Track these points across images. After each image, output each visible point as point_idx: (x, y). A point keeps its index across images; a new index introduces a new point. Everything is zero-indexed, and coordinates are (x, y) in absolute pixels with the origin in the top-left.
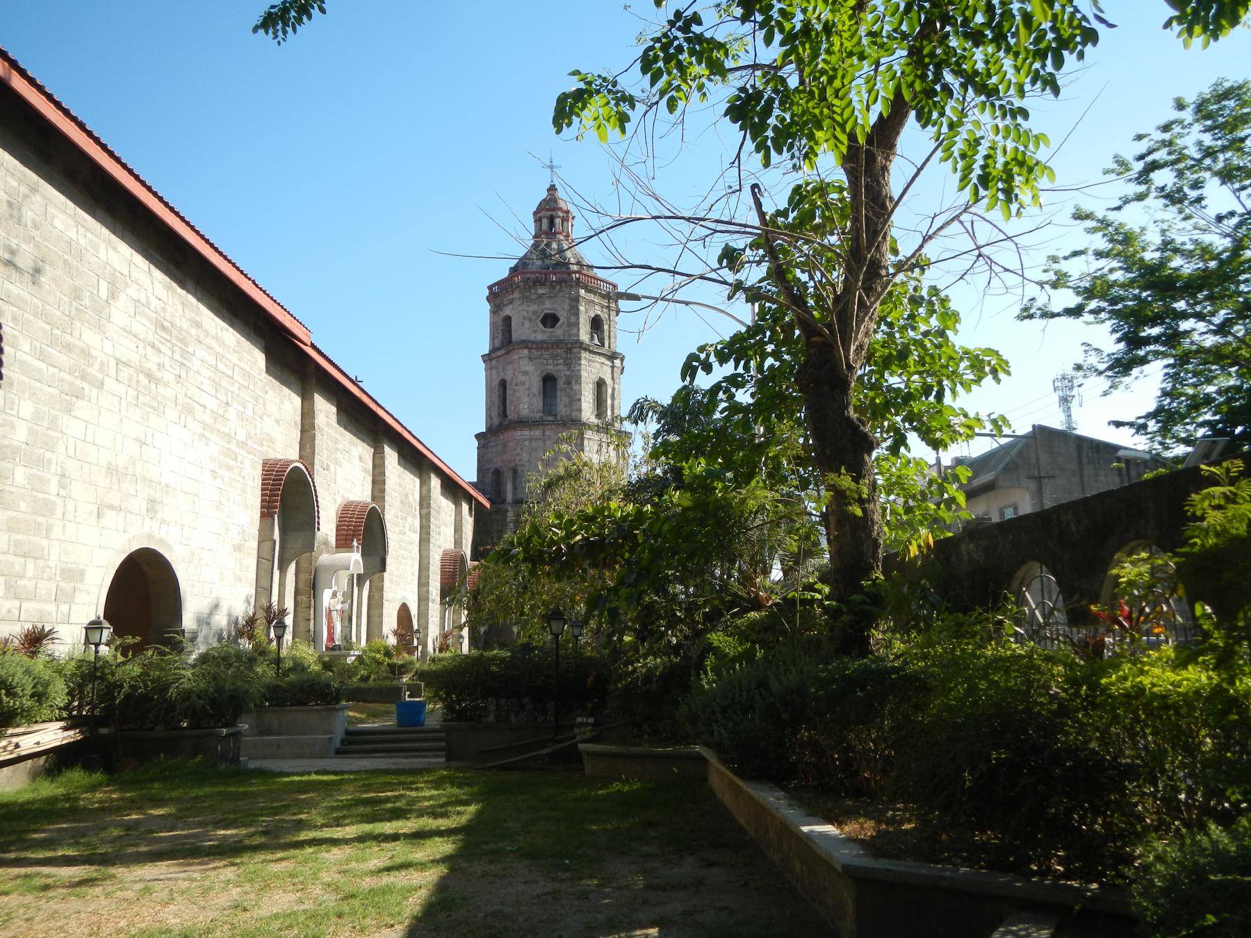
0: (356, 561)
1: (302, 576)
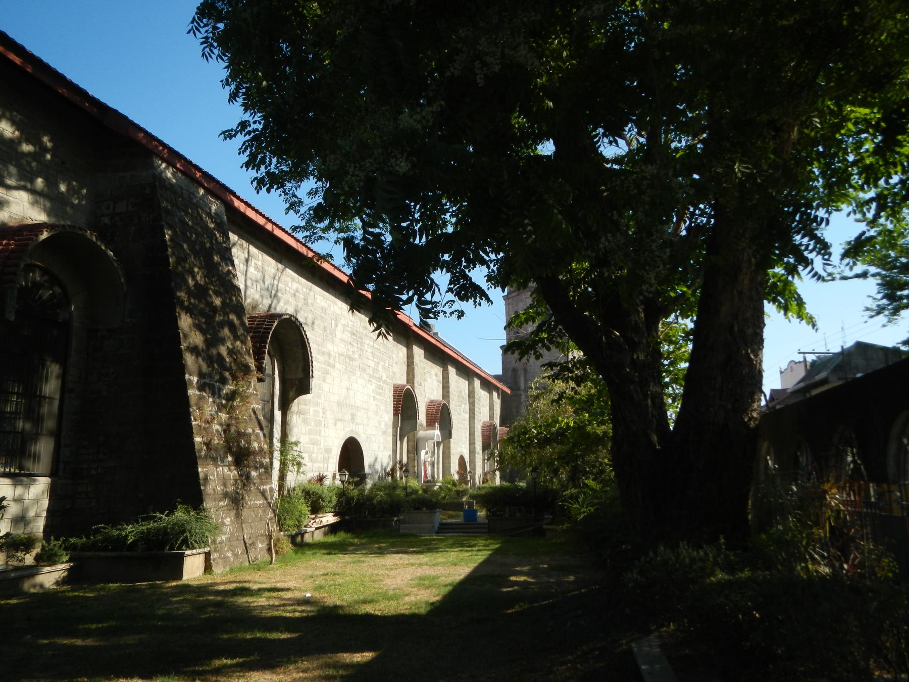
0: (438, 435)
1: (411, 443)
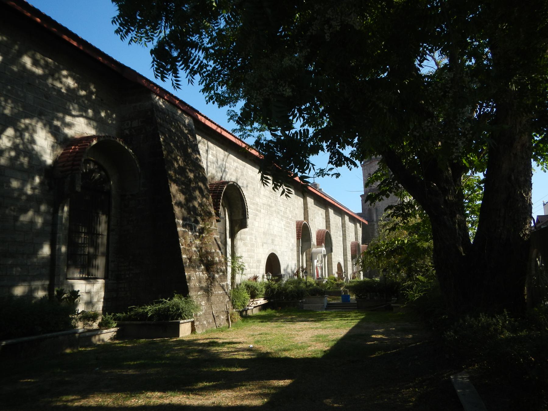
0: (324, 250)
1: (308, 256)
